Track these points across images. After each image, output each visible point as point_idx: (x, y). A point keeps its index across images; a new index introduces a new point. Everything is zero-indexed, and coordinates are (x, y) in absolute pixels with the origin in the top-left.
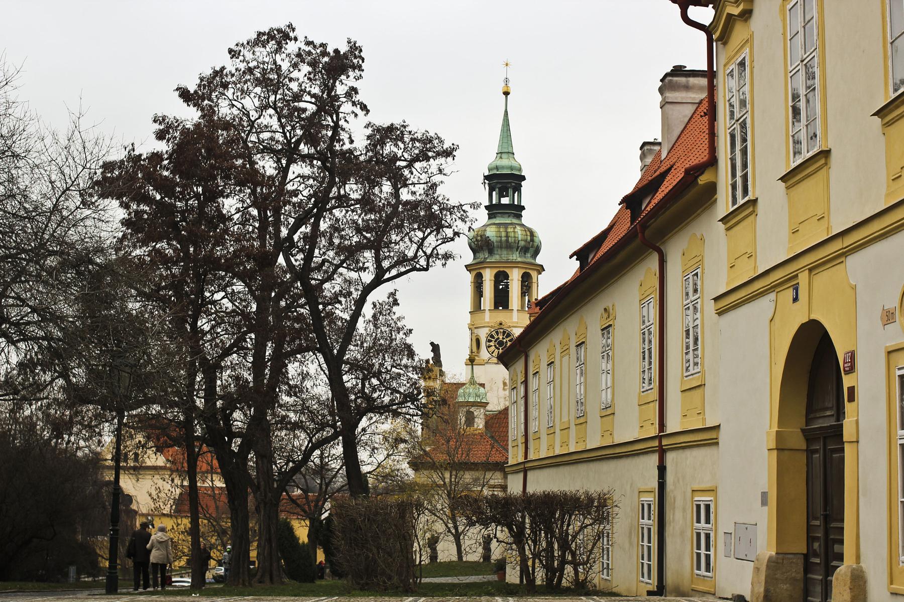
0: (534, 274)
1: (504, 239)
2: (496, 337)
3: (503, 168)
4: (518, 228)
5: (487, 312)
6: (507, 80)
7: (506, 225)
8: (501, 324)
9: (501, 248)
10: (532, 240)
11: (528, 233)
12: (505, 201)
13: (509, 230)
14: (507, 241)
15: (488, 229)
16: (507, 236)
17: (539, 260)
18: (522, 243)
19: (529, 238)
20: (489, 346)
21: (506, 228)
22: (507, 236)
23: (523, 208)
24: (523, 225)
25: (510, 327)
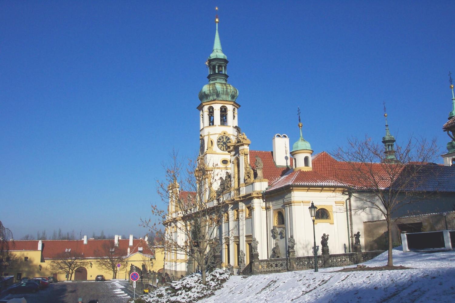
1: (225, 90)
5: (217, 126)
7: (225, 84)
8: (225, 133)
9: (223, 94)
13: (227, 86)
14: (227, 91)
16: (227, 88)
18: (233, 93)
19: (235, 92)
20: (219, 145)
22: (227, 88)
25: (229, 135)
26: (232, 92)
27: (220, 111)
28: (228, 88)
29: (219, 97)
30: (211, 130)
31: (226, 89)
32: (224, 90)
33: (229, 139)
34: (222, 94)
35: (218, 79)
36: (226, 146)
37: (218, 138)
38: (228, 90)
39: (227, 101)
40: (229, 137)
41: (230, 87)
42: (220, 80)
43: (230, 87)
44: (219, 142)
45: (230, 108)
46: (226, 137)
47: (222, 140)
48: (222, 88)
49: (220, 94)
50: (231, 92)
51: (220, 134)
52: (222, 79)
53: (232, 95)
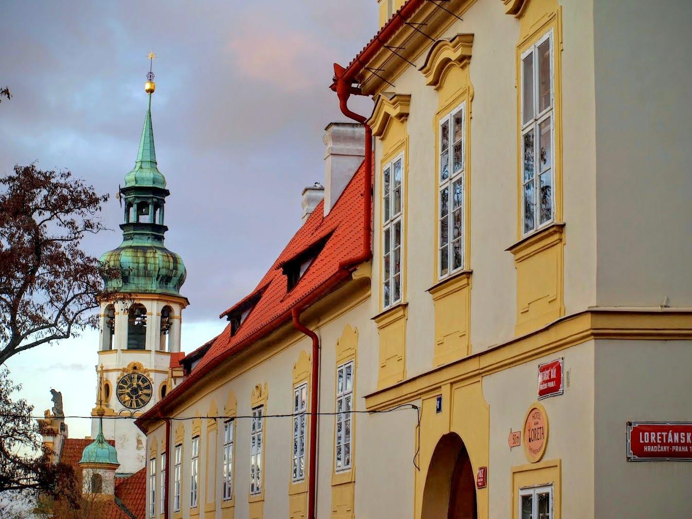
0: (176, 308)
1: (142, 265)
2: (129, 383)
3: (143, 179)
4: (159, 254)
6: (151, 77)
7: (144, 249)
8: (135, 368)
9: (138, 276)
10: (176, 268)
11: (171, 260)
12: (145, 219)
14: (145, 268)
15: (123, 253)
16: (146, 263)
17: (183, 292)
18: (164, 272)
19: (172, 266)
21: (145, 253)
22: (146, 263)
23: (166, 229)
24: (163, 249)
25: (145, 371)
26: (157, 269)
27: (126, 317)
28: (148, 261)
29: (129, 283)
30: (111, 361)
31: (144, 265)
32: (138, 267)
33: (145, 380)
34: (134, 275)
35: (136, 236)
36: (136, 398)
37: (118, 379)
38: (149, 265)
39: (145, 292)
40: (145, 375)
41: (154, 257)
42: (140, 239)
43: (154, 257)
44: (119, 387)
45: (153, 309)
46: (139, 378)
47: (129, 383)
48: (134, 263)
49: (131, 277)
50: (155, 270)
51: (124, 370)
52: (147, 237)
53: (159, 276)
